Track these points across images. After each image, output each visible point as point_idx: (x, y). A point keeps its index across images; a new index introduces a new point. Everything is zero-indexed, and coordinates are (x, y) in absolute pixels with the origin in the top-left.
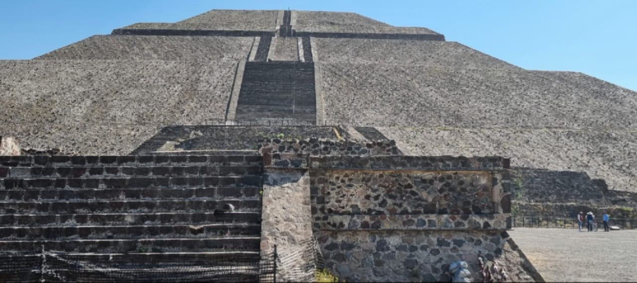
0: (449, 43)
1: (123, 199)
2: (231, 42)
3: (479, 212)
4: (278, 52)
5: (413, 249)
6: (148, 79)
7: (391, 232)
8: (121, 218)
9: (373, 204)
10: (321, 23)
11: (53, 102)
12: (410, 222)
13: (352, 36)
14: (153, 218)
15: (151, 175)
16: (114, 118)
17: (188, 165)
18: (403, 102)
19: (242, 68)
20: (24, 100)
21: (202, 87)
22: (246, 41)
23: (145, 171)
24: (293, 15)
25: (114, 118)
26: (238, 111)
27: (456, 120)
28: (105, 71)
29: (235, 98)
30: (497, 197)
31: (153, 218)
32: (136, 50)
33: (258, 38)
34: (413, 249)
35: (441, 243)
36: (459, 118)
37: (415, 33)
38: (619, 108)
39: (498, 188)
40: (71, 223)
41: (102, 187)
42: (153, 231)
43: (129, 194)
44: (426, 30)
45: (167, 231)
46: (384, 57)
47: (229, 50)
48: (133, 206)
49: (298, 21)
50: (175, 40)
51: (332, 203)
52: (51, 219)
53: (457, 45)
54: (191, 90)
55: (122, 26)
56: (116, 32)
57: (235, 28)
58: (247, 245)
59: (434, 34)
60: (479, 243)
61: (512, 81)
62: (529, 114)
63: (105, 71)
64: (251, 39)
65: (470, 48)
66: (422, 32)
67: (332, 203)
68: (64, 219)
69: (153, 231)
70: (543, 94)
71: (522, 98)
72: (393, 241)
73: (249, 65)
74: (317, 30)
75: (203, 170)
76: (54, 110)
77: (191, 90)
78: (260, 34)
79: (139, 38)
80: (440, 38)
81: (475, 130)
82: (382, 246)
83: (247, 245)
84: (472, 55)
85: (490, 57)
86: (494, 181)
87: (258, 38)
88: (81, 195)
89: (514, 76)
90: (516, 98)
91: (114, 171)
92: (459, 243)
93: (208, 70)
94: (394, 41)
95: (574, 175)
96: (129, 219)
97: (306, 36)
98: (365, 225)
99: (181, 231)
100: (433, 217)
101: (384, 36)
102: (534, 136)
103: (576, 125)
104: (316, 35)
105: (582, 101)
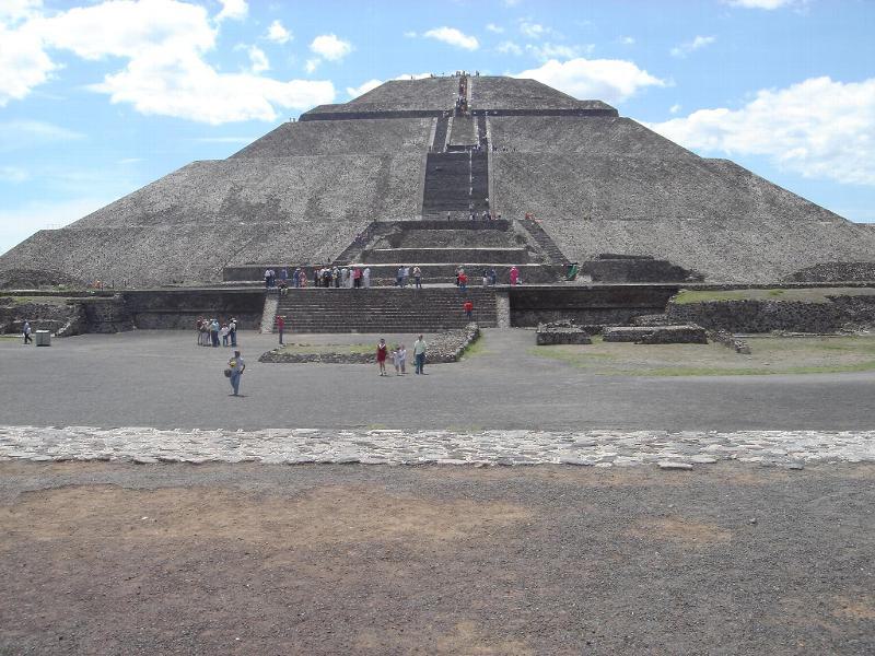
2: (411, 125)
10: (497, 96)
11: (279, 201)
19: (425, 161)
20: (254, 201)
21: (393, 182)
22: (424, 122)
24: (470, 84)
26: (424, 205)
27: (607, 211)
29: (422, 192)
33: (435, 119)
36: (607, 208)
37: (588, 108)
38: (745, 197)
44: (601, 103)
46: (556, 137)
47: (410, 134)
49: (474, 94)
50: (356, 124)
53: (628, 121)
56: (304, 117)
57: (411, 108)
66: (596, 107)
73: (431, 158)
78: (438, 113)
79: (327, 123)
80: (611, 112)
87: (435, 119)
93: (395, 164)
94: (566, 118)
101: (557, 113)
104: (491, 113)
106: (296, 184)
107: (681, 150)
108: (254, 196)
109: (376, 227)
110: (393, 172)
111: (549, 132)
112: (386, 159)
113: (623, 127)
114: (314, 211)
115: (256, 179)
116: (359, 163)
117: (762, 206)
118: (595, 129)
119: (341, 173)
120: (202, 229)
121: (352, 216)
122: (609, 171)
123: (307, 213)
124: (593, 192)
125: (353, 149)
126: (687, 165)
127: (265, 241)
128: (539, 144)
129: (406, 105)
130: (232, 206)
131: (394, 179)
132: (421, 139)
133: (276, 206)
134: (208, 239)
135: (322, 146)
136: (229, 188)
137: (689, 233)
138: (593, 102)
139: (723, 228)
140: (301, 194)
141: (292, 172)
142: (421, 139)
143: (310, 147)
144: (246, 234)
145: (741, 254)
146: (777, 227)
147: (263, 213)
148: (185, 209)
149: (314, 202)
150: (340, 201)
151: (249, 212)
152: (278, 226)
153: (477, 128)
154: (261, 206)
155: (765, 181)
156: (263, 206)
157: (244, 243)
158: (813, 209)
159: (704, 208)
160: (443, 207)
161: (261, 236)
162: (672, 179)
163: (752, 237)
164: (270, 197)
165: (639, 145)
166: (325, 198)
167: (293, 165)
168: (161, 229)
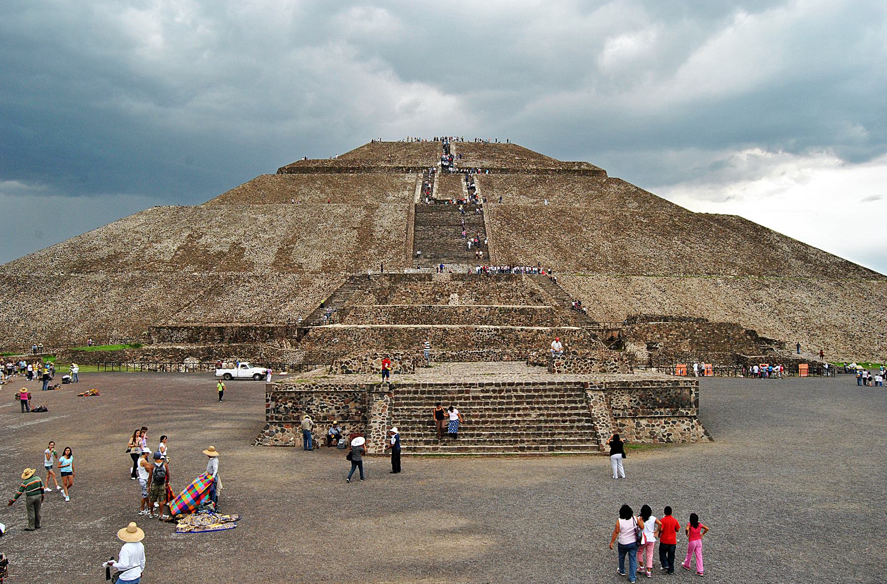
0: (611, 181)
1: (525, 405)
3: (683, 407)
4: (443, 189)
5: (653, 426)
7: (642, 418)
8: (529, 415)
9: (633, 404)
10: (482, 157)
11: (244, 249)
12: (652, 413)
13: (515, 171)
14: (543, 415)
15: (532, 393)
17: (548, 387)
18: (572, 247)
19: (413, 211)
22: (410, 178)
23: (529, 391)
24: (453, 148)
25: (301, 267)
27: (624, 267)
30: (692, 400)
31: (543, 415)
32: (305, 191)
34: (653, 426)
35: (666, 423)
37: (576, 168)
39: (693, 395)
40: (509, 418)
41: (514, 400)
42: (546, 421)
43: (528, 403)
44: (588, 165)
45: (552, 421)
46: (549, 194)
47: (396, 188)
48: (533, 409)
51: (614, 404)
52: (500, 416)
53: (619, 181)
54: (366, 235)
55: (287, 163)
56: (280, 171)
57: (396, 164)
58: (589, 428)
60: (683, 422)
62: (690, 260)
64: (414, 175)
65: (632, 186)
67: (614, 404)
68: (506, 416)
69: (546, 421)
71: (683, 243)
72: (643, 422)
75: (557, 390)
76: (245, 259)
77: (366, 235)
79: (305, 176)
81: (641, 278)
82: (638, 424)
83: (589, 428)
84: (634, 193)
86: (691, 392)
88: (507, 403)
90: (679, 242)
91: (516, 391)
92: (674, 423)
95: (732, 326)
96: (534, 415)
97: (467, 172)
98: (630, 414)
99: (558, 421)
100: (662, 410)
102: (693, 282)
107: (680, 209)
108: (214, 241)
109: (359, 281)
111: (541, 189)
112: (371, 208)
113: (615, 186)
114: (284, 260)
115: (219, 227)
116: (339, 211)
117: (796, 263)
118: (589, 188)
120: (144, 282)
121: (328, 268)
122: (618, 227)
124: (606, 247)
126: (699, 220)
127: (219, 294)
129: (389, 161)
130: (189, 253)
131: (377, 229)
132: (406, 193)
133: (240, 255)
134: (151, 294)
137: (731, 292)
138: (581, 164)
139: (767, 286)
141: (261, 218)
142: (406, 193)
143: (284, 197)
144: (198, 285)
145: (798, 316)
146: (825, 285)
148: (130, 258)
149: (284, 252)
150: (315, 251)
151: (207, 261)
152: (238, 277)
154: (221, 255)
155: (786, 237)
157: (192, 297)
158: (848, 266)
159: (736, 265)
161: (217, 290)
162: (689, 234)
163: (801, 295)
164: (235, 245)
165: (636, 204)
166: (299, 247)
167: (264, 213)
168: (92, 277)
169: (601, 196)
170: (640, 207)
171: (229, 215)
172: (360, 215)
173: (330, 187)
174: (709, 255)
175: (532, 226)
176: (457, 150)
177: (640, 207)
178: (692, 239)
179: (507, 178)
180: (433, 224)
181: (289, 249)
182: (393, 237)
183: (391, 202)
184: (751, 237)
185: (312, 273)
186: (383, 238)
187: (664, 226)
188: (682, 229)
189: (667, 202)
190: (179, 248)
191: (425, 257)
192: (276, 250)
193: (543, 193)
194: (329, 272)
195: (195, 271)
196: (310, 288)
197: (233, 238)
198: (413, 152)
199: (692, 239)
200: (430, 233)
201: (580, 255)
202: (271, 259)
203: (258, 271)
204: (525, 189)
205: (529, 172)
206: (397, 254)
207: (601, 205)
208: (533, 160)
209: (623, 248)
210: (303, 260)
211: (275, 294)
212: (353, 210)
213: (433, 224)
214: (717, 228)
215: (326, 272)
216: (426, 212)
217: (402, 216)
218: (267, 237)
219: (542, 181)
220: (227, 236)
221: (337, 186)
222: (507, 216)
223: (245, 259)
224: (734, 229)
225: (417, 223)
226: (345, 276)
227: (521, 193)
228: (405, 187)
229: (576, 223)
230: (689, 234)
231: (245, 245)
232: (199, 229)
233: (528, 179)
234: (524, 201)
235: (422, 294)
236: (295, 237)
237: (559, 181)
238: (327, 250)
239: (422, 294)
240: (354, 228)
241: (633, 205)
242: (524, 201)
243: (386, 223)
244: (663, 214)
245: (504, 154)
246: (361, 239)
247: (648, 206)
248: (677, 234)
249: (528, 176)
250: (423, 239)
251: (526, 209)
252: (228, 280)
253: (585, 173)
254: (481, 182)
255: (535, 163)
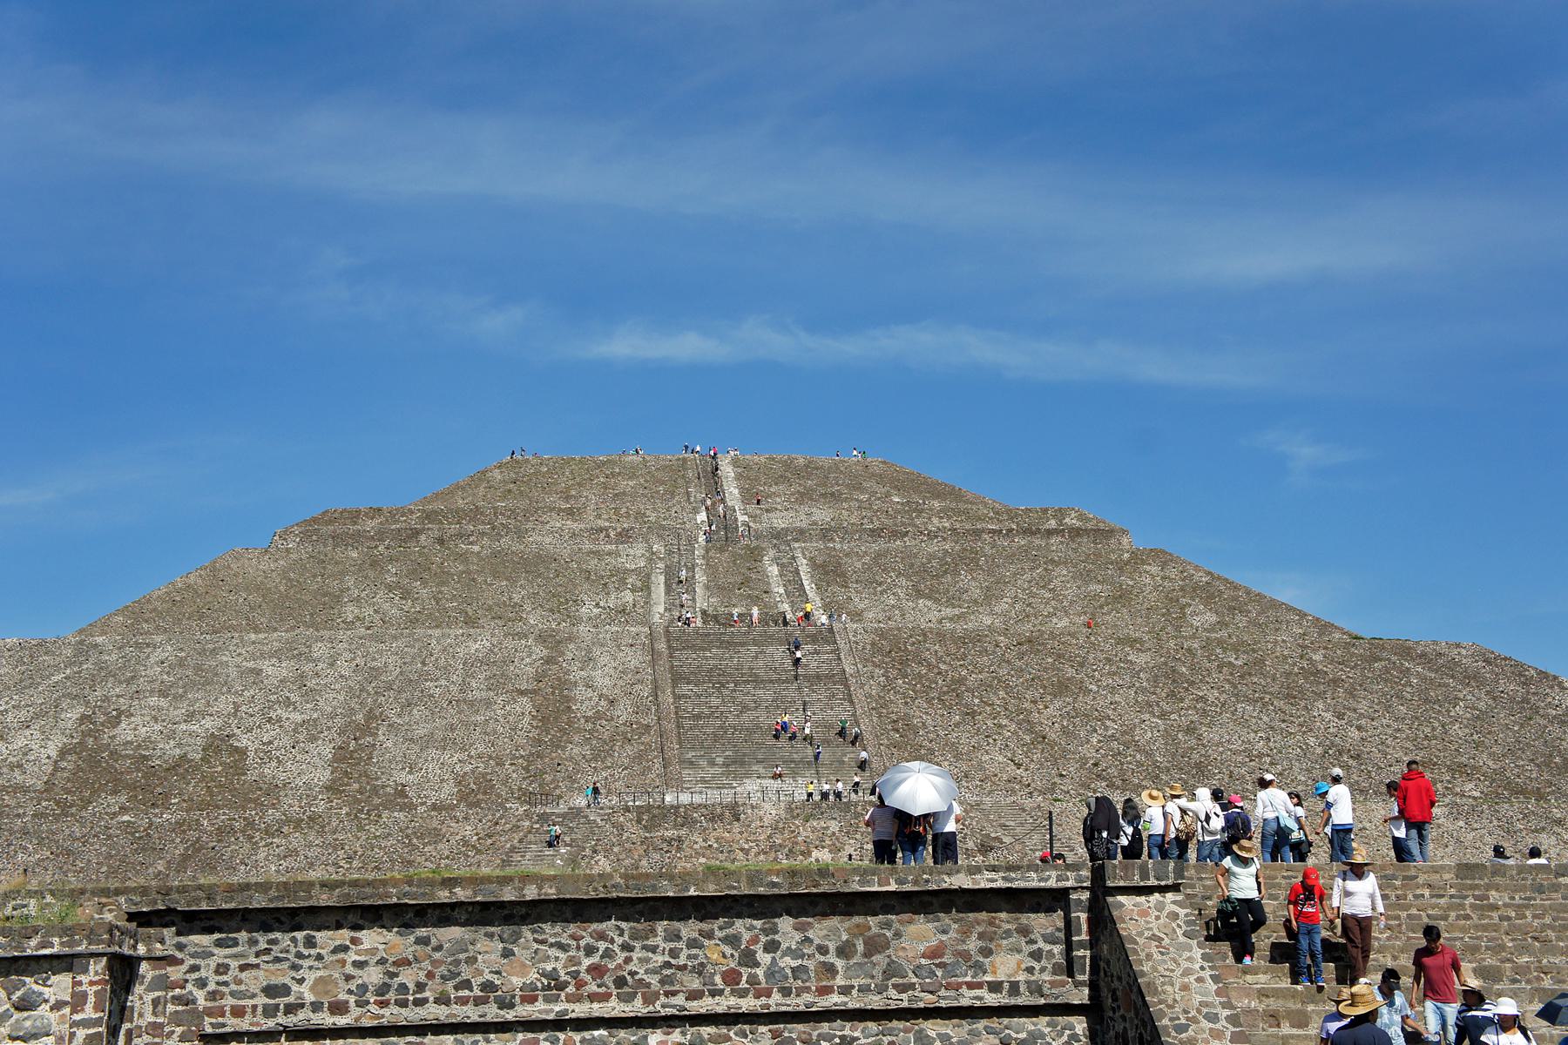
2: (593, 563)
6: (443, 682)
10: (804, 497)
11: (242, 752)
13: (896, 534)
16: (401, 792)
19: (662, 646)
20: (171, 750)
21: (585, 703)
22: (633, 556)
25: (401, 792)
28: (332, 665)
37: (1053, 523)
46: (990, 596)
49: (742, 490)
59: (1102, 526)
61: (1314, 673)
63: (336, 662)
64: (639, 549)
65: (1197, 568)
70: (1388, 708)
71: (1340, 716)
74: (802, 522)
76: (251, 776)
77: (554, 709)
85: (1248, 592)
89: (1317, 657)
90: (1328, 716)
97: (778, 535)
101: (977, 533)
103: (1471, 786)
104: (801, 534)
105: (1480, 719)
106: (288, 703)
110: (577, 674)
111: (970, 583)
112: (553, 642)
115: (163, 694)
118: (1086, 577)
119: (424, 676)
121: (476, 792)
123: (332, 788)
124: (1149, 731)
125: (440, 620)
128: (949, 611)
129: (570, 513)
130: (93, 766)
131: (580, 692)
132: (628, 597)
135: (350, 612)
136: (72, 715)
140: (312, 732)
141: (273, 670)
147: (193, 788)
149: (351, 760)
150: (433, 752)
151: (149, 781)
153: (774, 570)
156: (197, 768)
160: (738, 766)
164: (218, 744)
166: (388, 742)
167: (276, 654)
169: (1122, 597)
170: (1222, 624)
171: (181, 663)
172: (528, 661)
173: (425, 583)
174: (1409, 745)
175: (962, 681)
176: (739, 477)
177: (1222, 624)
178: (1363, 706)
179: (879, 555)
180: (718, 679)
181: (361, 748)
182: (623, 712)
183: (594, 621)
184: (1512, 700)
185: (434, 807)
186: (599, 716)
187: (1288, 674)
188: (1336, 682)
189: (1290, 609)
190: (63, 753)
191: (712, 763)
192: (327, 751)
193: (976, 593)
194: (477, 804)
195: (124, 810)
196: (440, 846)
197: (208, 723)
198: (627, 485)
199: (1363, 706)
200: (715, 701)
201: (1088, 751)
202: (323, 776)
203: (291, 805)
204: (929, 581)
205: (932, 536)
206: (639, 757)
207: (1118, 620)
208: (936, 504)
209: (1190, 730)
210: (403, 777)
211: (355, 864)
212: (509, 643)
213: (718, 679)
214: (1423, 679)
215: (470, 805)
216: (693, 648)
217: (635, 659)
218: (298, 717)
219: (968, 559)
220: (190, 717)
221: (443, 578)
222: (894, 651)
223: (251, 776)
224: (1471, 678)
225: (677, 678)
226: (527, 814)
227: (919, 594)
228: (623, 581)
229: (1070, 672)
230: (1351, 693)
231: (244, 741)
232: (106, 699)
233: (931, 557)
234: (928, 614)
235: (746, 852)
236: (370, 716)
237: (1011, 558)
238: (463, 749)
239: (746, 852)
240: (522, 693)
241: (1202, 617)
242: (928, 614)
243: (602, 679)
244: (1285, 639)
245: (862, 490)
246: (544, 720)
247: (1242, 622)
248: (1320, 695)
249: (933, 547)
250: (698, 717)
251: (941, 637)
252: (223, 832)
253: (1076, 533)
254: (812, 562)
255: (944, 513)
